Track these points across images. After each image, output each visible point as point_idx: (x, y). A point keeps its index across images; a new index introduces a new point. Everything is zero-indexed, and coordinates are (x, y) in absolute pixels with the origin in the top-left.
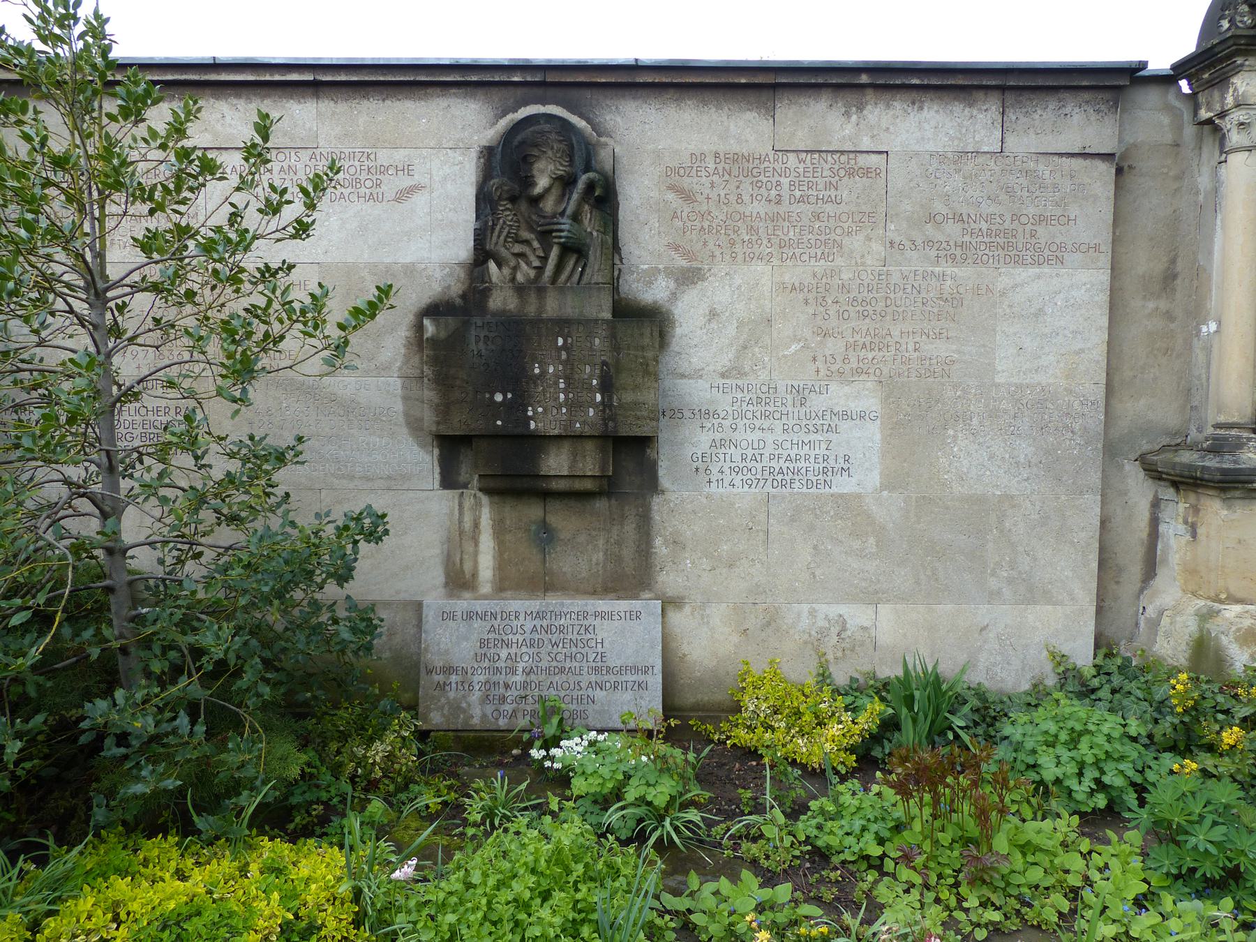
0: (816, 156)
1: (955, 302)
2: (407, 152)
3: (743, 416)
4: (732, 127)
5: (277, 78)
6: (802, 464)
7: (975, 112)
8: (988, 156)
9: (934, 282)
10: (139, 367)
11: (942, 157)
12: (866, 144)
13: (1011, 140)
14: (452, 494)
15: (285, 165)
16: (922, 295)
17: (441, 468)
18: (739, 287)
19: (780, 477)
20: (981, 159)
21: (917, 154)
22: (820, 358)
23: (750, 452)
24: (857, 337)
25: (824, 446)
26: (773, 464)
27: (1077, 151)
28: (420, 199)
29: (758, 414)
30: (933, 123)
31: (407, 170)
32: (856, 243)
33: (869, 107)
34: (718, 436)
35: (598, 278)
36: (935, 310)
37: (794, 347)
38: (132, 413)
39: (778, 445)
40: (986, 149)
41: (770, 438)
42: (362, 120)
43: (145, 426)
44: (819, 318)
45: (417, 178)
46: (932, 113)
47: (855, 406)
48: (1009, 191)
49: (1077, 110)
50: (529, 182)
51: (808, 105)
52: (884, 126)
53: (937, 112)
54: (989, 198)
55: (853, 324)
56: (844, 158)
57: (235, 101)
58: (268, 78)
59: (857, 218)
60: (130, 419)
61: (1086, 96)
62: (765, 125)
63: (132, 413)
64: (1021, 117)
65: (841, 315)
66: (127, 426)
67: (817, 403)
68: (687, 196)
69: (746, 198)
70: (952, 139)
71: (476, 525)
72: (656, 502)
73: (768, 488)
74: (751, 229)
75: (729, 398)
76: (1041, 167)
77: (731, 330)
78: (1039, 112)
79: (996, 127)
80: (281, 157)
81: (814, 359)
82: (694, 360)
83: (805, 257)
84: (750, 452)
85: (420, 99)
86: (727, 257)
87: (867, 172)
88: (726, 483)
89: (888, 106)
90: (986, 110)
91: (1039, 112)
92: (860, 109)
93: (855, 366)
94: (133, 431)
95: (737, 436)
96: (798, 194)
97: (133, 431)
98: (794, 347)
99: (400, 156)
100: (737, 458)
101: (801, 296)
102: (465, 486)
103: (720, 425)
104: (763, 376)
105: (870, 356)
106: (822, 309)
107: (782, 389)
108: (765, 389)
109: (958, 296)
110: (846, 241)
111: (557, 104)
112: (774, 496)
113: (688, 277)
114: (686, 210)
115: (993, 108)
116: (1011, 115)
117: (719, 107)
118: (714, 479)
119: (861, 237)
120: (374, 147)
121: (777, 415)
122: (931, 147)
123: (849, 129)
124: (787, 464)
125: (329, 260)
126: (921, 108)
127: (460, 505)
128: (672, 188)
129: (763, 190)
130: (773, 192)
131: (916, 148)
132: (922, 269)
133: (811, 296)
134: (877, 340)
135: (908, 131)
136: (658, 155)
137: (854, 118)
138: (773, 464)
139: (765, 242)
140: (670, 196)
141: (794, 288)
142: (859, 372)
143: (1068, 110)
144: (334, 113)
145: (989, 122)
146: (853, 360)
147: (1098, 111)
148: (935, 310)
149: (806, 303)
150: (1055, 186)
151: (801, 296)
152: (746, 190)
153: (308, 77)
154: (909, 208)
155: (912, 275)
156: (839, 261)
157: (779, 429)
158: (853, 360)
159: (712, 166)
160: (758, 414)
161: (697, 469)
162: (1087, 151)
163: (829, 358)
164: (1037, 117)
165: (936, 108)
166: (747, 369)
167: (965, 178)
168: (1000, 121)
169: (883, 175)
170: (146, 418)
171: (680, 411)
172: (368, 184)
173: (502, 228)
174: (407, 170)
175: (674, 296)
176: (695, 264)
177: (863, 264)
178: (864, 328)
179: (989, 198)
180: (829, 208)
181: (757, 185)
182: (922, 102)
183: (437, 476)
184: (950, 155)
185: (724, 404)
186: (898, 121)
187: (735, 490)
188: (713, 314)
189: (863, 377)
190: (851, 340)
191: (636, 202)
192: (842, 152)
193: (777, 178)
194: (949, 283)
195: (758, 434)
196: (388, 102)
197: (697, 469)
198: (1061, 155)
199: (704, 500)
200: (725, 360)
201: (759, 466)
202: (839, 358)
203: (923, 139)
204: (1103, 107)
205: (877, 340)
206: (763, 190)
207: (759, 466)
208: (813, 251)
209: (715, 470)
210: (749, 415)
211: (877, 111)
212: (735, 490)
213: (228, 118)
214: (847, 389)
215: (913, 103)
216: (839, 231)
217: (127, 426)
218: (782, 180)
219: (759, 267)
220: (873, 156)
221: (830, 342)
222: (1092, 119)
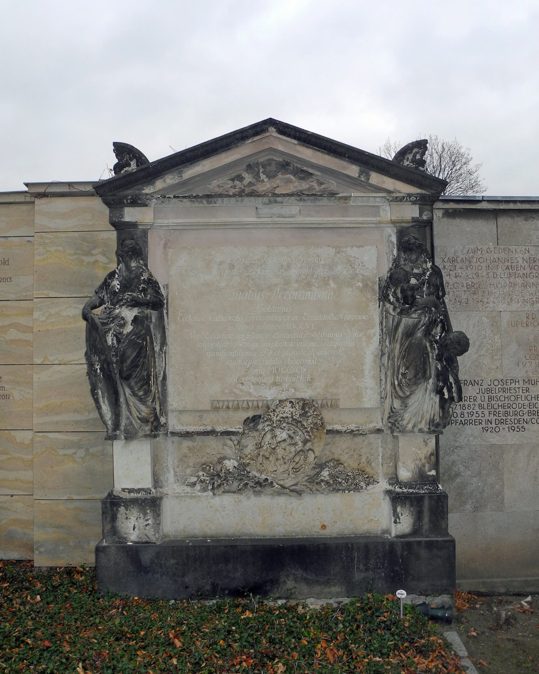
10: (527, 372)
38: (523, 399)
43: (531, 407)
60: (522, 402)
63: (523, 399)
66: (520, 407)
94: (524, 410)
97: (524, 410)
170: (531, 402)
217: (520, 407)
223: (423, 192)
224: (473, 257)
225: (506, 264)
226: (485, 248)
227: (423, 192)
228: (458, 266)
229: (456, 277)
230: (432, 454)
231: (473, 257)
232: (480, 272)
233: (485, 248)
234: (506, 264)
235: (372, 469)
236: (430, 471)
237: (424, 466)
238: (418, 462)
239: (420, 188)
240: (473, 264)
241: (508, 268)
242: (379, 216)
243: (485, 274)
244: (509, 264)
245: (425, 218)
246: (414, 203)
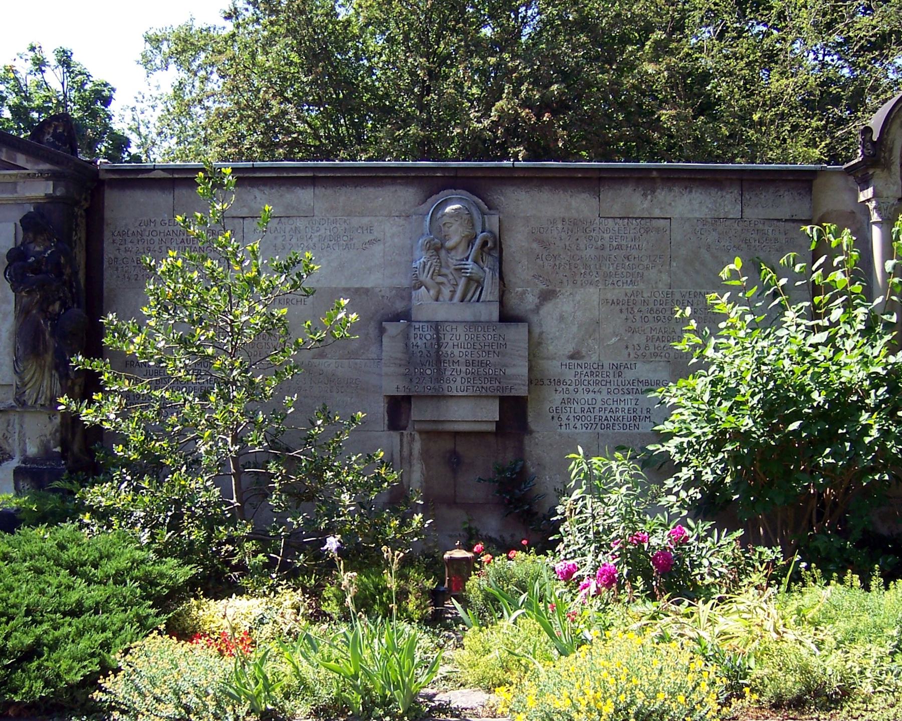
0: (626, 220)
2: (369, 218)
3: (581, 383)
4: (573, 203)
5: (291, 175)
6: (620, 414)
7: (724, 194)
11: (704, 221)
12: (657, 213)
13: (748, 212)
14: (395, 436)
15: (293, 227)
17: (389, 416)
18: (579, 302)
19: (606, 423)
20: (728, 223)
21: (689, 219)
22: (630, 346)
23: (586, 407)
24: (654, 333)
25: (634, 402)
26: (601, 414)
27: (788, 218)
28: (378, 248)
29: (591, 382)
31: (370, 229)
32: (652, 274)
33: (659, 190)
34: (566, 396)
35: (490, 298)
36: (703, 316)
37: (614, 340)
39: (604, 402)
40: (731, 216)
41: (599, 397)
42: (342, 199)
44: (629, 321)
45: (376, 234)
46: (698, 194)
47: (653, 377)
48: (746, 241)
49: (786, 193)
50: (445, 238)
51: (620, 189)
52: (668, 202)
55: (651, 325)
56: (643, 222)
57: (263, 188)
58: (285, 175)
59: (652, 259)
62: (594, 202)
65: (644, 319)
67: (629, 375)
68: (545, 244)
69: (582, 246)
70: (711, 210)
71: (411, 454)
72: (527, 439)
73: (598, 429)
74: (586, 266)
75: (573, 372)
76: (766, 228)
77: (575, 329)
80: (291, 222)
81: (627, 347)
82: (551, 348)
83: (620, 283)
84: (586, 407)
85: (378, 186)
86: (571, 283)
87: (658, 230)
88: (571, 427)
89: (670, 190)
92: (653, 192)
93: (652, 351)
95: (579, 396)
96: (615, 244)
98: (614, 340)
99: (365, 220)
100: (578, 410)
101: (618, 307)
102: (404, 428)
103: (568, 390)
104: (595, 358)
105: (662, 345)
106: (631, 316)
107: (606, 366)
108: (596, 366)
110: (646, 273)
111: (464, 189)
112: (602, 435)
113: (546, 296)
114: (545, 254)
117: (565, 191)
118: (563, 424)
119: (655, 271)
120: (348, 215)
121: (603, 383)
122: (697, 215)
123: (646, 205)
124: (611, 414)
125: (320, 286)
126: (691, 192)
127: (401, 440)
128: (535, 240)
129: (593, 241)
130: (599, 243)
131: (690, 216)
133: (624, 307)
134: (666, 335)
136: (527, 219)
137: (649, 197)
138: (601, 414)
139: (595, 274)
140: (535, 245)
141: (613, 302)
142: (655, 355)
143: (781, 193)
144: (324, 195)
146: (652, 347)
147: (800, 194)
148: (703, 316)
149: (621, 311)
150: (776, 239)
151: (618, 307)
152: (583, 243)
153: (310, 174)
154: (685, 252)
156: (642, 286)
157: (605, 392)
158: (652, 347)
159: (560, 226)
160: (591, 382)
161: (553, 418)
163: (637, 347)
166: (584, 354)
169: (668, 232)
171: (542, 380)
172: (345, 238)
173: (430, 267)
174: (370, 229)
175: (538, 308)
176: (550, 287)
177: (657, 287)
178: (658, 328)
180: (634, 253)
181: (590, 239)
183: (386, 422)
185: (569, 376)
187: (577, 431)
188: (562, 318)
189: (658, 359)
190: (650, 335)
191: (513, 249)
192: (642, 218)
193: (602, 234)
195: (591, 395)
196: (358, 188)
197: (553, 418)
198: (778, 220)
199: (557, 437)
200: (570, 348)
201: (592, 415)
202: (643, 347)
205: (666, 335)
206: (593, 241)
207: (592, 415)
208: (624, 279)
209: (564, 419)
210: (586, 383)
211: (663, 193)
212: (577, 431)
213: (258, 198)
214: (647, 366)
215: (686, 188)
216: (641, 267)
218: (605, 235)
219: (592, 290)
220: (662, 221)
221: (637, 335)
223: (56, 168)
224: (145, 230)
225: (181, 237)
226: (159, 220)
227: (56, 168)
228: (128, 239)
229: (126, 251)
230: (56, 431)
231: (145, 230)
232: (152, 246)
233: (159, 220)
234: (181, 237)
235: (9, 445)
236: (55, 447)
237: (49, 441)
238: (42, 438)
239: (52, 164)
240: (145, 238)
241: (183, 241)
242: (16, 192)
243: (157, 248)
244: (185, 237)
245: (58, 194)
246: (47, 179)
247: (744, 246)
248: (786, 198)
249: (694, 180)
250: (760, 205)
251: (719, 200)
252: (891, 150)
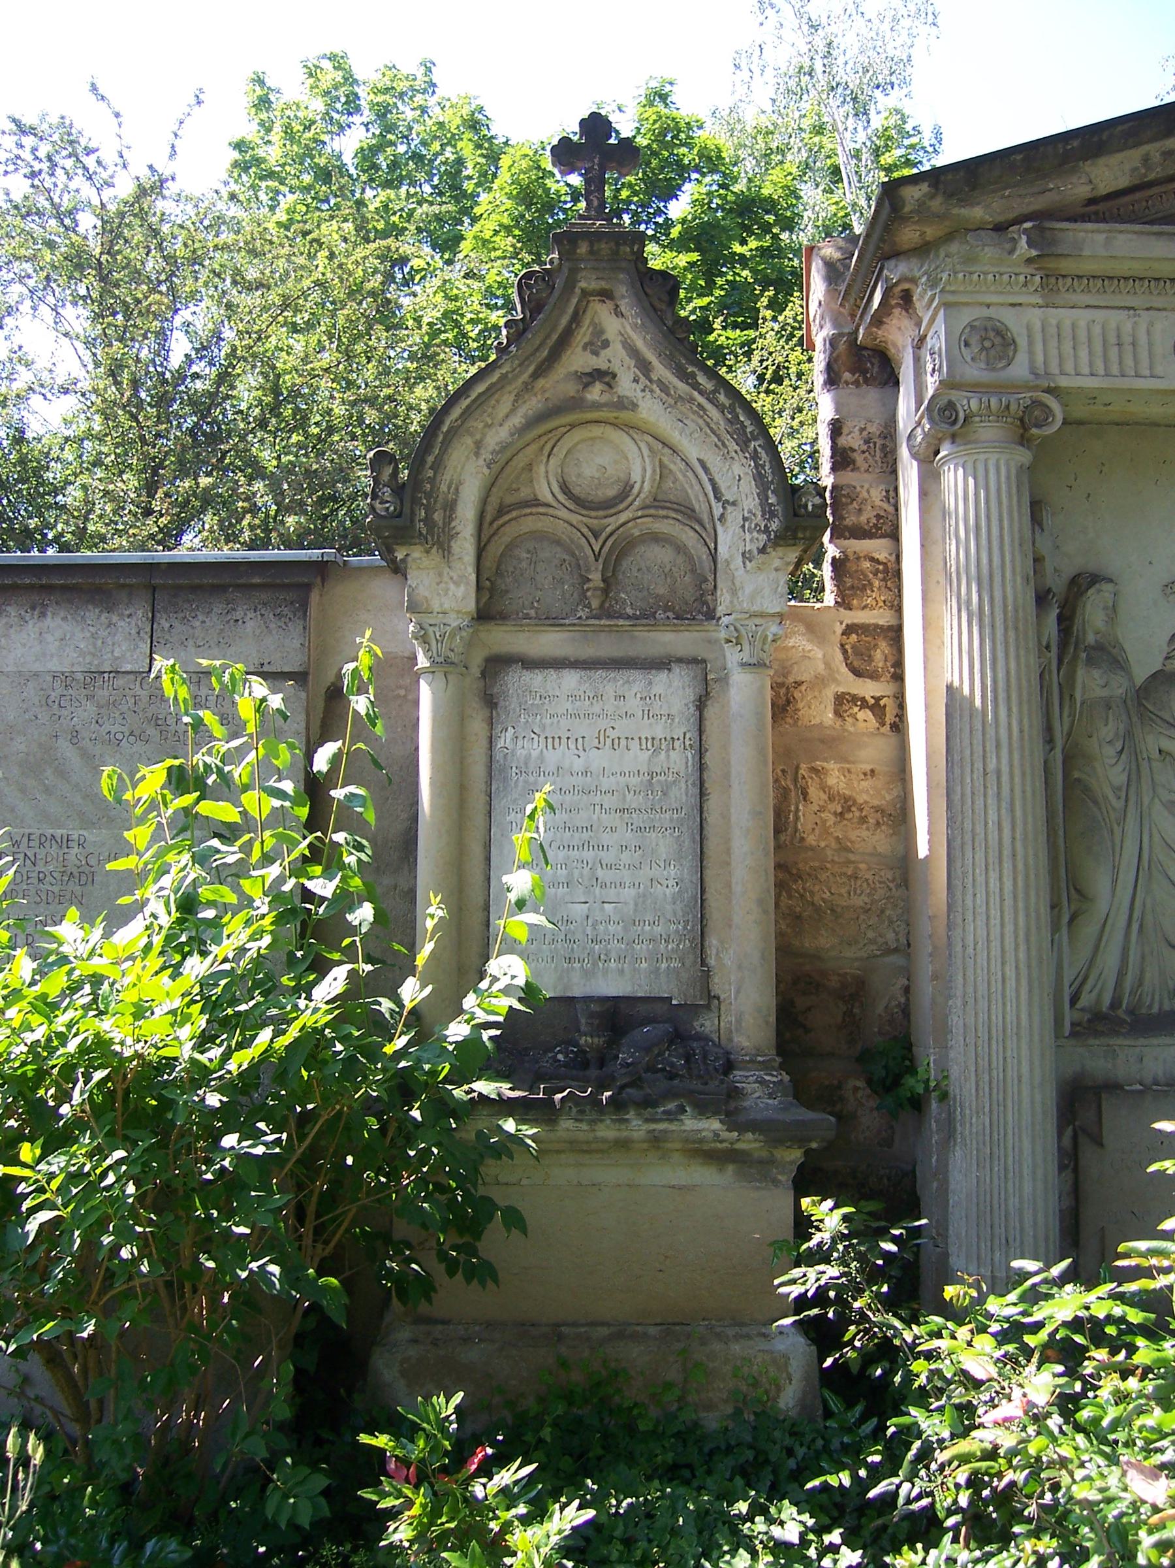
1: (84, 878)
7: (115, 618)
8: (132, 677)
9: (54, 851)
11: (67, 679)
16: (37, 869)
20: (120, 682)
21: (36, 674)
30: (58, 634)
36: (56, 889)
40: (128, 668)
46: (58, 621)
49: (251, 614)
53: (64, 619)
54: (131, 734)
61: (264, 596)
64: (176, 624)
70: (82, 654)
78: (201, 618)
79: (142, 639)
90: (130, 616)
91: (201, 618)
109: (87, 869)
115: (140, 613)
116: (163, 622)
122: (54, 665)
126: (43, 615)
131: (37, 667)
132: (39, 832)
135: (24, 645)
143: (239, 614)
145: (133, 632)
147: (278, 616)
154: (23, 748)
155: (25, 839)
162: (266, 669)
164: (198, 624)
165: (62, 614)
167: (99, 707)
168: (148, 629)
179: (131, 734)
182: (45, 606)
184: (80, 676)
186: (12, 631)
194: (76, 850)
203: (44, 655)
204: (286, 611)
215: (33, 608)
222: (272, 626)
247: (152, 731)
248: (250, 625)
249: (49, 589)
250: (191, 642)
251: (103, 633)
252: (450, 507)
